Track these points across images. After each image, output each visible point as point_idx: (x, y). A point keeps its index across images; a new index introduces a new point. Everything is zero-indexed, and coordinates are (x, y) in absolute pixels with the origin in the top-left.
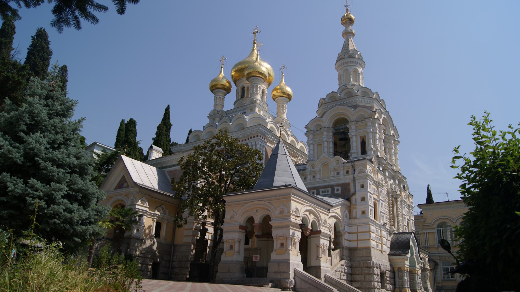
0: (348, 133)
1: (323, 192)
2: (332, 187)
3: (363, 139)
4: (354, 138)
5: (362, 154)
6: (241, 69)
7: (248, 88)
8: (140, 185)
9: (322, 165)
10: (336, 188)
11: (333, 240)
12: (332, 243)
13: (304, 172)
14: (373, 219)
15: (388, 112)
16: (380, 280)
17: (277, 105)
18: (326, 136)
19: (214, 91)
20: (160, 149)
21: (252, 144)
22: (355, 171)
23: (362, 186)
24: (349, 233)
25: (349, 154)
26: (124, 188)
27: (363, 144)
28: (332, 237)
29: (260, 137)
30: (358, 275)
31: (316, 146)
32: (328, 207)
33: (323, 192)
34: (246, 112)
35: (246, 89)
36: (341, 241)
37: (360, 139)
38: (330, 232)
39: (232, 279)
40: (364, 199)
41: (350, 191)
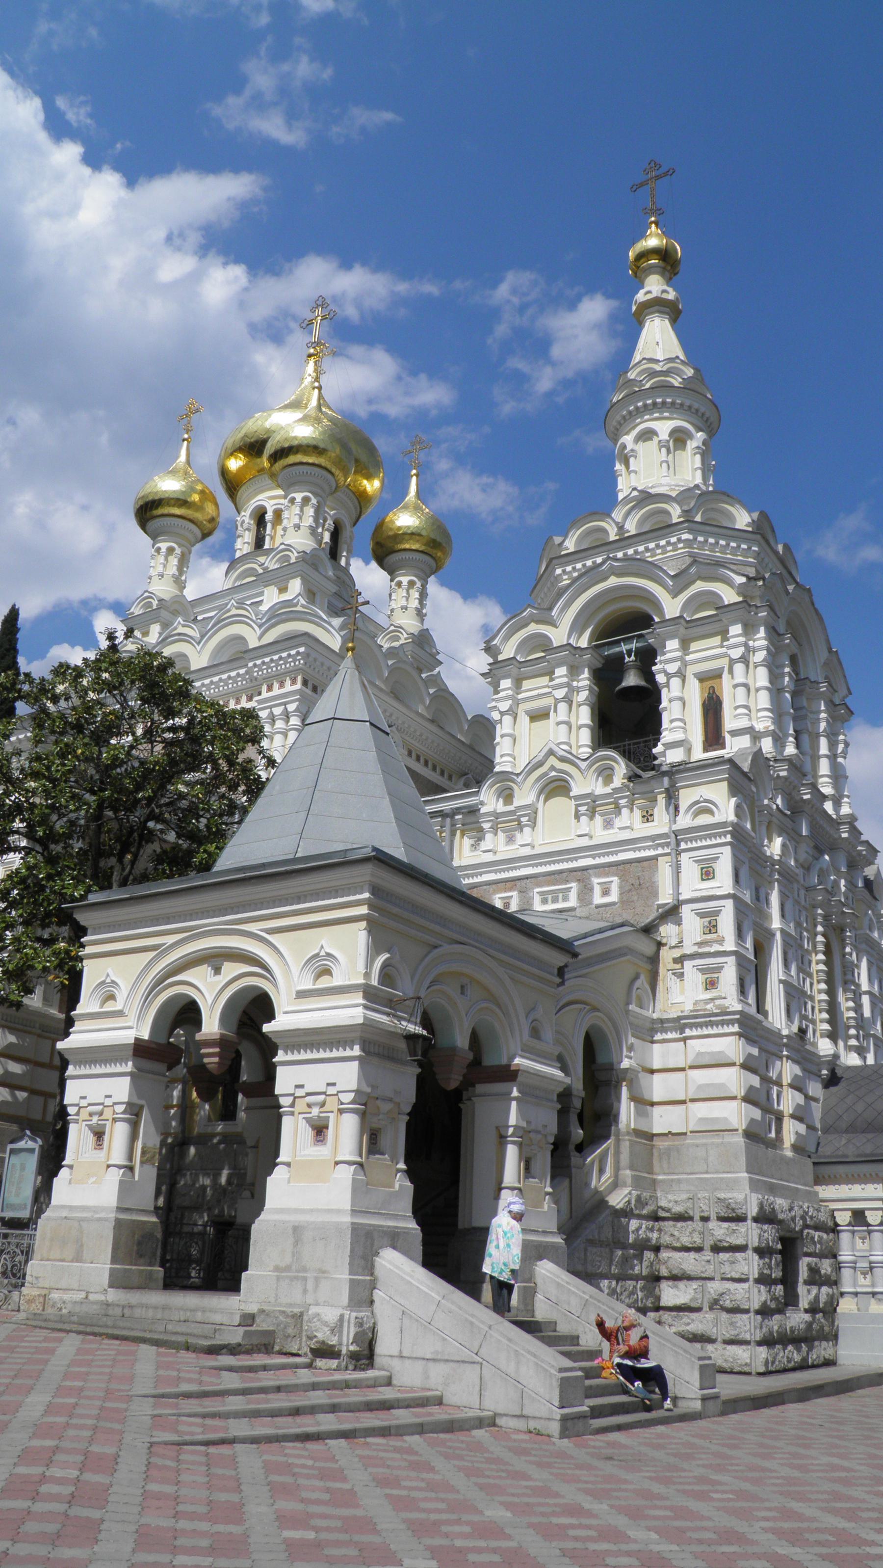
0: (654, 668)
1: (544, 901)
2: (582, 875)
3: (713, 687)
5: (706, 750)
6: (257, 442)
7: (278, 514)
9: (540, 792)
10: (596, 881)
11: (577, 1104)
12: (574, 1119)
13: (471, 819)
14: (753, 1010)
15: (809, 590)
16: (777, 1274)
17: (392, 580)
18: (565, 680)
19: (152, 525)
21: (272, 713)
22: (677, 809)
23: (707, 873)
24: (652, 1072)
25: (655, 751)
28: (575, 1092)
29: (305, 683)
30: (687, 1249)
31: (524, 719)
32: (558, 959)
33: (544, 901)
34: (262, 601)
35: (269, 516)
36: (615, 1104)
37: (702, 689)
38: (564, 1069)
39: (92, 1297)
40: (715, 926)
41: (655, 894)
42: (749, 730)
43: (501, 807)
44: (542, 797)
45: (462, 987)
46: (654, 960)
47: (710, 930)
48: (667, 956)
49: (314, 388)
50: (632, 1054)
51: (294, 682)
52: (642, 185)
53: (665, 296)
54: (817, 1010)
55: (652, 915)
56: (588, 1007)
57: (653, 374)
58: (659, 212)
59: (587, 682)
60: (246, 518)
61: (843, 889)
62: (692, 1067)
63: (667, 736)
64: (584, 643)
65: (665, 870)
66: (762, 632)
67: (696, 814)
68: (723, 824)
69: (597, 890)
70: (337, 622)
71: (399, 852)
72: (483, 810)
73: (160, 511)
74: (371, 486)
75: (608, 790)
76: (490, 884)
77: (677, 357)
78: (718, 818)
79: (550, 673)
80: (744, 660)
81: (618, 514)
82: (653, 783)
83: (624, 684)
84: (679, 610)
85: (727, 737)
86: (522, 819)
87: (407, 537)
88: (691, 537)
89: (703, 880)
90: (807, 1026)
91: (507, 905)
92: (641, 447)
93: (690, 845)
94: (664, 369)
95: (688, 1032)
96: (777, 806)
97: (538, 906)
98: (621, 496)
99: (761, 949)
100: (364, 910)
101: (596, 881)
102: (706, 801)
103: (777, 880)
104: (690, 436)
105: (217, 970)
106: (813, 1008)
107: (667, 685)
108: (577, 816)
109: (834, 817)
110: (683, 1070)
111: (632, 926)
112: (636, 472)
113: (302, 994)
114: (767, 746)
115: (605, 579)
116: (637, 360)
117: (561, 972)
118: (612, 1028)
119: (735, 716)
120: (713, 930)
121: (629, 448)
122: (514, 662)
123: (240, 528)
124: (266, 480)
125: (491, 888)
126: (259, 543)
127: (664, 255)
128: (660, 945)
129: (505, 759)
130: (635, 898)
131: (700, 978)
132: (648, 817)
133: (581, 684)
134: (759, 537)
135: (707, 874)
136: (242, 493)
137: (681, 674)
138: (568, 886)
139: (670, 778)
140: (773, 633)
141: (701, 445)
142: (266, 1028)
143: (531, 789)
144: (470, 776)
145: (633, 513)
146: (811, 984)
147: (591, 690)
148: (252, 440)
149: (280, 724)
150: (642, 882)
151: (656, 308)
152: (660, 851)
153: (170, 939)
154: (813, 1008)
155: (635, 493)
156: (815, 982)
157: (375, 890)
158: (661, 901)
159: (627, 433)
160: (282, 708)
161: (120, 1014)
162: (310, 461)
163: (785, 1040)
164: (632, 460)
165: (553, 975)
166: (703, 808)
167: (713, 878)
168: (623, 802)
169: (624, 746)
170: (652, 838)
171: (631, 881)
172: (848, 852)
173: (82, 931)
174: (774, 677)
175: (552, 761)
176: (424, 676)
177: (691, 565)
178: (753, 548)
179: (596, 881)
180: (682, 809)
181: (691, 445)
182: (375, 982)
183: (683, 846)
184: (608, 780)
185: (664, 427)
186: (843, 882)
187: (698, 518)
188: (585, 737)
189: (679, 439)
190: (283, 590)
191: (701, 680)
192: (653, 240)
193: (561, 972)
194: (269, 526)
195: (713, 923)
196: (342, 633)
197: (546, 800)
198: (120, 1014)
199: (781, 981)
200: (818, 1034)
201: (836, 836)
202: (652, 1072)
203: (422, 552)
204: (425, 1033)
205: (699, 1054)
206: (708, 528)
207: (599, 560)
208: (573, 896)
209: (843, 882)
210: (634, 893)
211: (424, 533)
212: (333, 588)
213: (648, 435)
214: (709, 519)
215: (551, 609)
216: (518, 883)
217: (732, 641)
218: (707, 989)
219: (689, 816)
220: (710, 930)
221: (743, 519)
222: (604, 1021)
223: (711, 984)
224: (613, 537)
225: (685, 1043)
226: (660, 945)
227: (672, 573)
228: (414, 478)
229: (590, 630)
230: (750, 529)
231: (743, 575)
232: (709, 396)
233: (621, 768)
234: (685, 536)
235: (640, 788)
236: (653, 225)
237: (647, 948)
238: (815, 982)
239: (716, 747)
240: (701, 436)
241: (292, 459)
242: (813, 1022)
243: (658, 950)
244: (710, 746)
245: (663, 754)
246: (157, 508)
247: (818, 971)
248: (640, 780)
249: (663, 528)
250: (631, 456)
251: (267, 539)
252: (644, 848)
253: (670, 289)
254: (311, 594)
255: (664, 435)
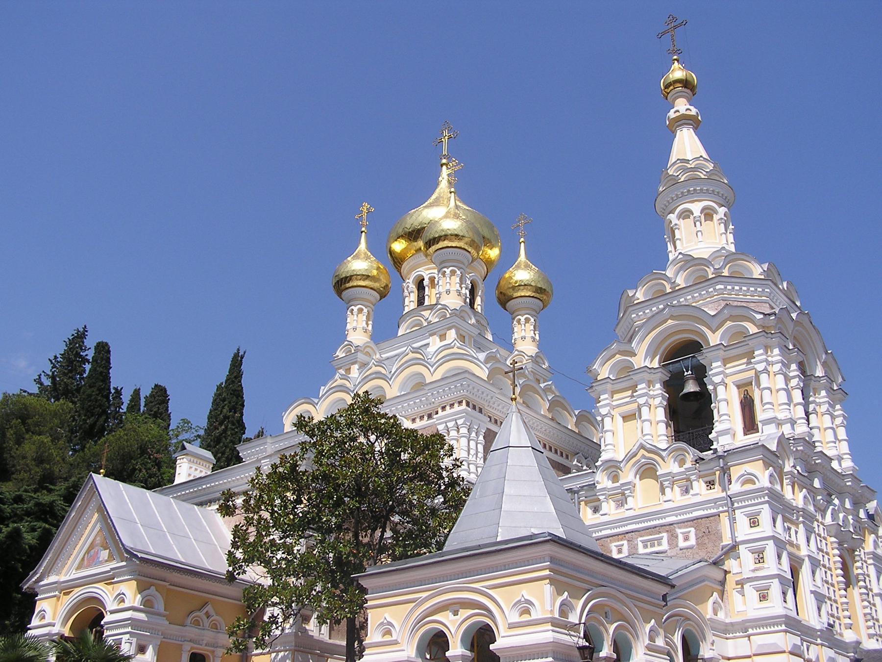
4: (721, 389)
5: (745, 434)
6: (413, 231)
7: (432, 280)
8: (140, 555)
13: (592, 493)
20: (208, 454)
22: (730, 482)
23: (754, 523)
25: (710, 436)
26: (101, 563)
27: (748, 406)
29: (468, 404)
32: (663, 590)
33: (645, 547)
34: (429, 344)
35: (426, 282)
37: (739, 392)
41: (720, 539)
42: (773, 420)
43: (609, 484)
44: (638, 476)
45: (606, 613)
46: (723, 583)
47: (759, 561)
48: (731, 580)
49: (451, 193)
50: (714, 648)
51: (460, 403)
52: (664, 33)
53: (688, 113)
54: (840, 610)
55: (720, 553)
56: (682, 618)
57: (685, 170)
58: (678, 52)
59: (660, 392)
60: (410, 284)
61: (851, 521)
62: (755, 655)
63: (718, 427)
64: (655, 364)
65: (725, 520)
66: (776, 351)
67: (743, 484)
68: (761, 489)
69: (681, 537)
70: (482, 356)
71: (560, 533)
72: (599, 487)
73: (351, 284)
74: (493, 253)
75: (682, 469)
76: (608, 537)
77: (701, 156)
78: (758, 485)
79: (634, 388)
80: (766, 371)
81: (670, 273)
82: (712, 464)
83: (685, 391)
84: (719, 339)
85: (760, 425)
86: (626, 492)
87: (522, 288)
88: (722, 287)
89: (751, 527)
90: (834, 622)
91: (620, 551)
92: (681, 222)
93: (740, 504)
94: (693, 166)
95: (750, 631)
96: (798, 471)
97: (641, 550)
98: (671, 257)
99: (795, 572)
100: (547, 572)
101: (679, 531)
102: (749, 474)
103: (803, 522)
104: (716, 212)
105: (456, 613)
106: (837, 608)
107: (715, 389)
108: (663, 491)
109: (840, 471)
110: (749, 657)
111: (706, 561)
112: (680, 240)
113: (512, 626)
114: (787, 429)
115: (665, 321)
116: (673, 161)
117: (664, 597)
118: (700, 633)
119: (764, 410)
120: (761, 561)
121: (673, 224)
122: (608, 380)
123: (406, 291)
124: (421, 257)
125: (608, 540)
126: (421, 301)
127: (686, 83)
128: (726, 572)
129: (608, 447)
130: (707, 541)
131: (756, 595)
132: (710, 484)
133: (656, 393)
134: (770, 283)
135: (754, 522)
136: (405, 267)
137: (723, 383)
138: (661, 535)
139: (723, 460)
140: (784, 349)
141: (723, 217)
142: (492, 647)
143: (630, 470)
144: (580, 454)
145: (680, 274)
146: (834, 591)
147: (663, 397)
148: (410, 230)
149: (453, 433)
150: (710, 530)
151: (683, 121)
152: (721, 509)
153: (425, 595)
154: (837, 608)
155: (680, 256)
156: (837, 590)
157: (552, 560)
158: (724, 543)
159: (672, 212)
160: (454, 422)
161: (395, 643)
162: (454, 245)
163: (819, 633)
164: (676, 231)
165: (660, 600)
166: (749, 479)
167: (758, 525)
168: (693, 477)
169: (689, 433)
170: (715, 501)
171: (703, 530)
172: (853, 495)
173: (364, 591)
174: (787, 379)
175: (642, 452)
176: (542, 385)
177: (724, 308)
178: (766, 290)
179: (679, 531)
180: (733, 482)
181: (716, 217)
182: (557, 616)
183: (736, 505)
184: (682, 463)
185: (696, 208)
186: (850, 517)
187: (726, 273)
188: (662, 428)
189: (708, 214)
190: (443, 337)
191: (738, 387)
192: (678, 72)
193: (664, 597)
194: (427, 289)
195: (761, 556)
196: (488, 366)
197: (641, 479)
198: (395, 643)
199: (812, 592)
200: (843, 627)
201: (842, 484)
202: (729, 659)
203: (533, 297)
204: (587, 644)
205: (760, 646)
206: (733, 280)
207: (661, 307)
208: (665, 541)
209: (850, 517)
210: (706, 538)
211: (533, 284)
212: (477, 331)
213: (686, 214)
214: (734, 272)
215: (630, 341)
216: (627, 535)
217: (757, 359)
218: (761, 601)
219: (739, 484)
220: (759, 561)
221: (757, 270)
222: (694, 627)
223: (763, 598)
224: (669, 290)
225: (749, 640)
226: (726, 572)
227: (712, 313)
228: (522, 244)
229: (658, 357)
230: (762, 277)
231: (761, 313)
232: (726, 182)
233: (691, 454)
234: (718, 287)
235: (703, 468)
236: (676, 62)
237: (717, 574)
238: (837, 590)
239: (752, 431)
240: (722, 210)
241: (441, 244)
242: (838, 618)
243: (726, 576)
244: (748, 431)
245: (717, 438)
246: (349, 282)
247: (838, 583)
248: (703, 462)
249: (701, 282)
250: (676, 228)
251: (426, 298)
252: (710, 508)
253: (692, 108)
254: (461, 337)
255: (697, 213)
